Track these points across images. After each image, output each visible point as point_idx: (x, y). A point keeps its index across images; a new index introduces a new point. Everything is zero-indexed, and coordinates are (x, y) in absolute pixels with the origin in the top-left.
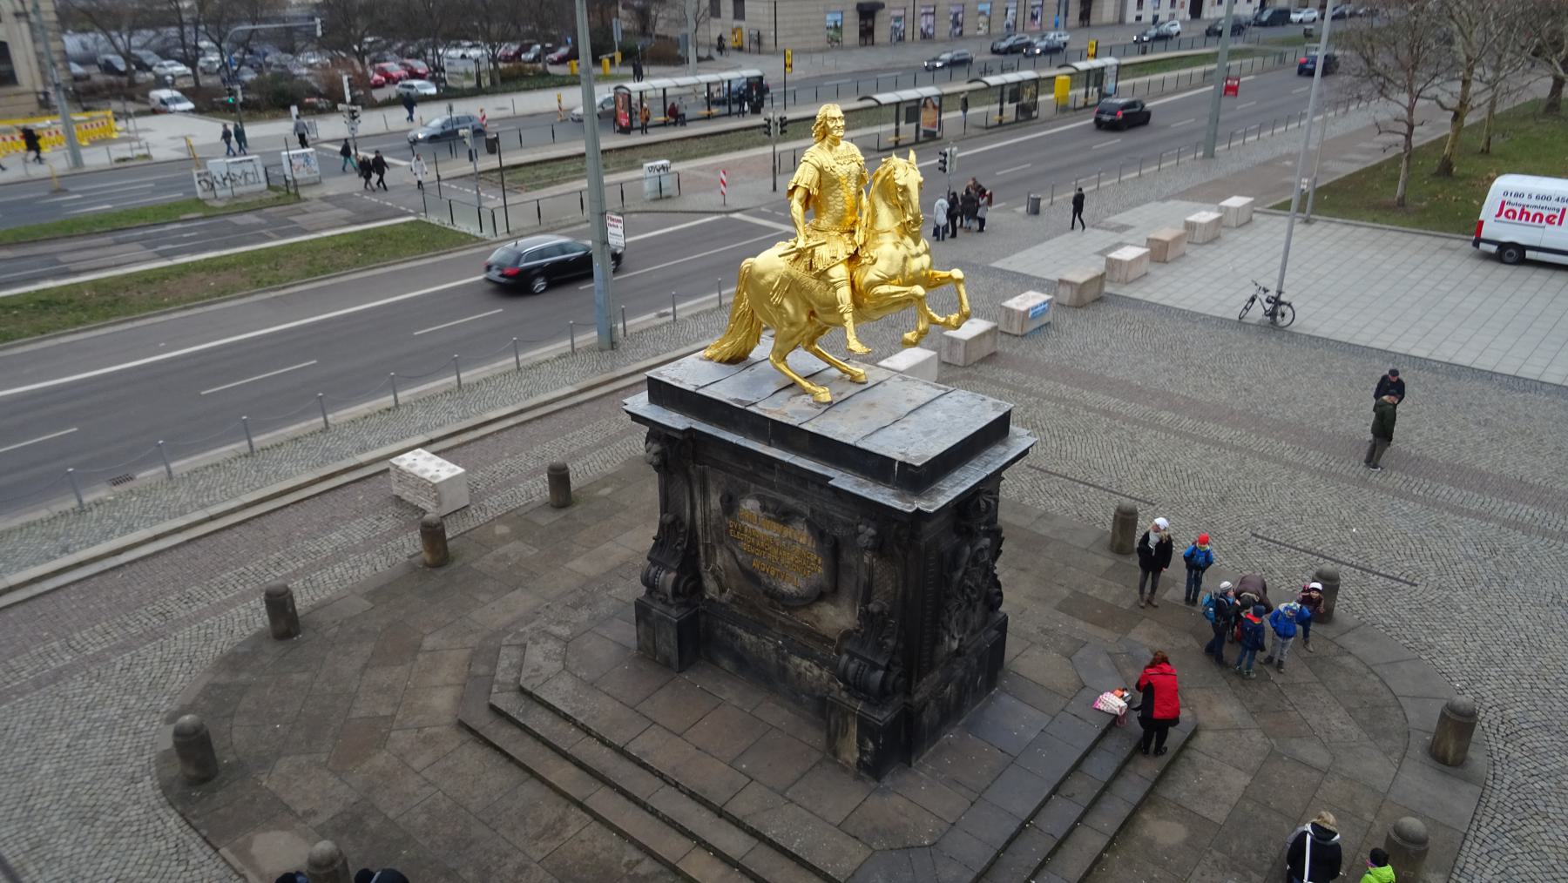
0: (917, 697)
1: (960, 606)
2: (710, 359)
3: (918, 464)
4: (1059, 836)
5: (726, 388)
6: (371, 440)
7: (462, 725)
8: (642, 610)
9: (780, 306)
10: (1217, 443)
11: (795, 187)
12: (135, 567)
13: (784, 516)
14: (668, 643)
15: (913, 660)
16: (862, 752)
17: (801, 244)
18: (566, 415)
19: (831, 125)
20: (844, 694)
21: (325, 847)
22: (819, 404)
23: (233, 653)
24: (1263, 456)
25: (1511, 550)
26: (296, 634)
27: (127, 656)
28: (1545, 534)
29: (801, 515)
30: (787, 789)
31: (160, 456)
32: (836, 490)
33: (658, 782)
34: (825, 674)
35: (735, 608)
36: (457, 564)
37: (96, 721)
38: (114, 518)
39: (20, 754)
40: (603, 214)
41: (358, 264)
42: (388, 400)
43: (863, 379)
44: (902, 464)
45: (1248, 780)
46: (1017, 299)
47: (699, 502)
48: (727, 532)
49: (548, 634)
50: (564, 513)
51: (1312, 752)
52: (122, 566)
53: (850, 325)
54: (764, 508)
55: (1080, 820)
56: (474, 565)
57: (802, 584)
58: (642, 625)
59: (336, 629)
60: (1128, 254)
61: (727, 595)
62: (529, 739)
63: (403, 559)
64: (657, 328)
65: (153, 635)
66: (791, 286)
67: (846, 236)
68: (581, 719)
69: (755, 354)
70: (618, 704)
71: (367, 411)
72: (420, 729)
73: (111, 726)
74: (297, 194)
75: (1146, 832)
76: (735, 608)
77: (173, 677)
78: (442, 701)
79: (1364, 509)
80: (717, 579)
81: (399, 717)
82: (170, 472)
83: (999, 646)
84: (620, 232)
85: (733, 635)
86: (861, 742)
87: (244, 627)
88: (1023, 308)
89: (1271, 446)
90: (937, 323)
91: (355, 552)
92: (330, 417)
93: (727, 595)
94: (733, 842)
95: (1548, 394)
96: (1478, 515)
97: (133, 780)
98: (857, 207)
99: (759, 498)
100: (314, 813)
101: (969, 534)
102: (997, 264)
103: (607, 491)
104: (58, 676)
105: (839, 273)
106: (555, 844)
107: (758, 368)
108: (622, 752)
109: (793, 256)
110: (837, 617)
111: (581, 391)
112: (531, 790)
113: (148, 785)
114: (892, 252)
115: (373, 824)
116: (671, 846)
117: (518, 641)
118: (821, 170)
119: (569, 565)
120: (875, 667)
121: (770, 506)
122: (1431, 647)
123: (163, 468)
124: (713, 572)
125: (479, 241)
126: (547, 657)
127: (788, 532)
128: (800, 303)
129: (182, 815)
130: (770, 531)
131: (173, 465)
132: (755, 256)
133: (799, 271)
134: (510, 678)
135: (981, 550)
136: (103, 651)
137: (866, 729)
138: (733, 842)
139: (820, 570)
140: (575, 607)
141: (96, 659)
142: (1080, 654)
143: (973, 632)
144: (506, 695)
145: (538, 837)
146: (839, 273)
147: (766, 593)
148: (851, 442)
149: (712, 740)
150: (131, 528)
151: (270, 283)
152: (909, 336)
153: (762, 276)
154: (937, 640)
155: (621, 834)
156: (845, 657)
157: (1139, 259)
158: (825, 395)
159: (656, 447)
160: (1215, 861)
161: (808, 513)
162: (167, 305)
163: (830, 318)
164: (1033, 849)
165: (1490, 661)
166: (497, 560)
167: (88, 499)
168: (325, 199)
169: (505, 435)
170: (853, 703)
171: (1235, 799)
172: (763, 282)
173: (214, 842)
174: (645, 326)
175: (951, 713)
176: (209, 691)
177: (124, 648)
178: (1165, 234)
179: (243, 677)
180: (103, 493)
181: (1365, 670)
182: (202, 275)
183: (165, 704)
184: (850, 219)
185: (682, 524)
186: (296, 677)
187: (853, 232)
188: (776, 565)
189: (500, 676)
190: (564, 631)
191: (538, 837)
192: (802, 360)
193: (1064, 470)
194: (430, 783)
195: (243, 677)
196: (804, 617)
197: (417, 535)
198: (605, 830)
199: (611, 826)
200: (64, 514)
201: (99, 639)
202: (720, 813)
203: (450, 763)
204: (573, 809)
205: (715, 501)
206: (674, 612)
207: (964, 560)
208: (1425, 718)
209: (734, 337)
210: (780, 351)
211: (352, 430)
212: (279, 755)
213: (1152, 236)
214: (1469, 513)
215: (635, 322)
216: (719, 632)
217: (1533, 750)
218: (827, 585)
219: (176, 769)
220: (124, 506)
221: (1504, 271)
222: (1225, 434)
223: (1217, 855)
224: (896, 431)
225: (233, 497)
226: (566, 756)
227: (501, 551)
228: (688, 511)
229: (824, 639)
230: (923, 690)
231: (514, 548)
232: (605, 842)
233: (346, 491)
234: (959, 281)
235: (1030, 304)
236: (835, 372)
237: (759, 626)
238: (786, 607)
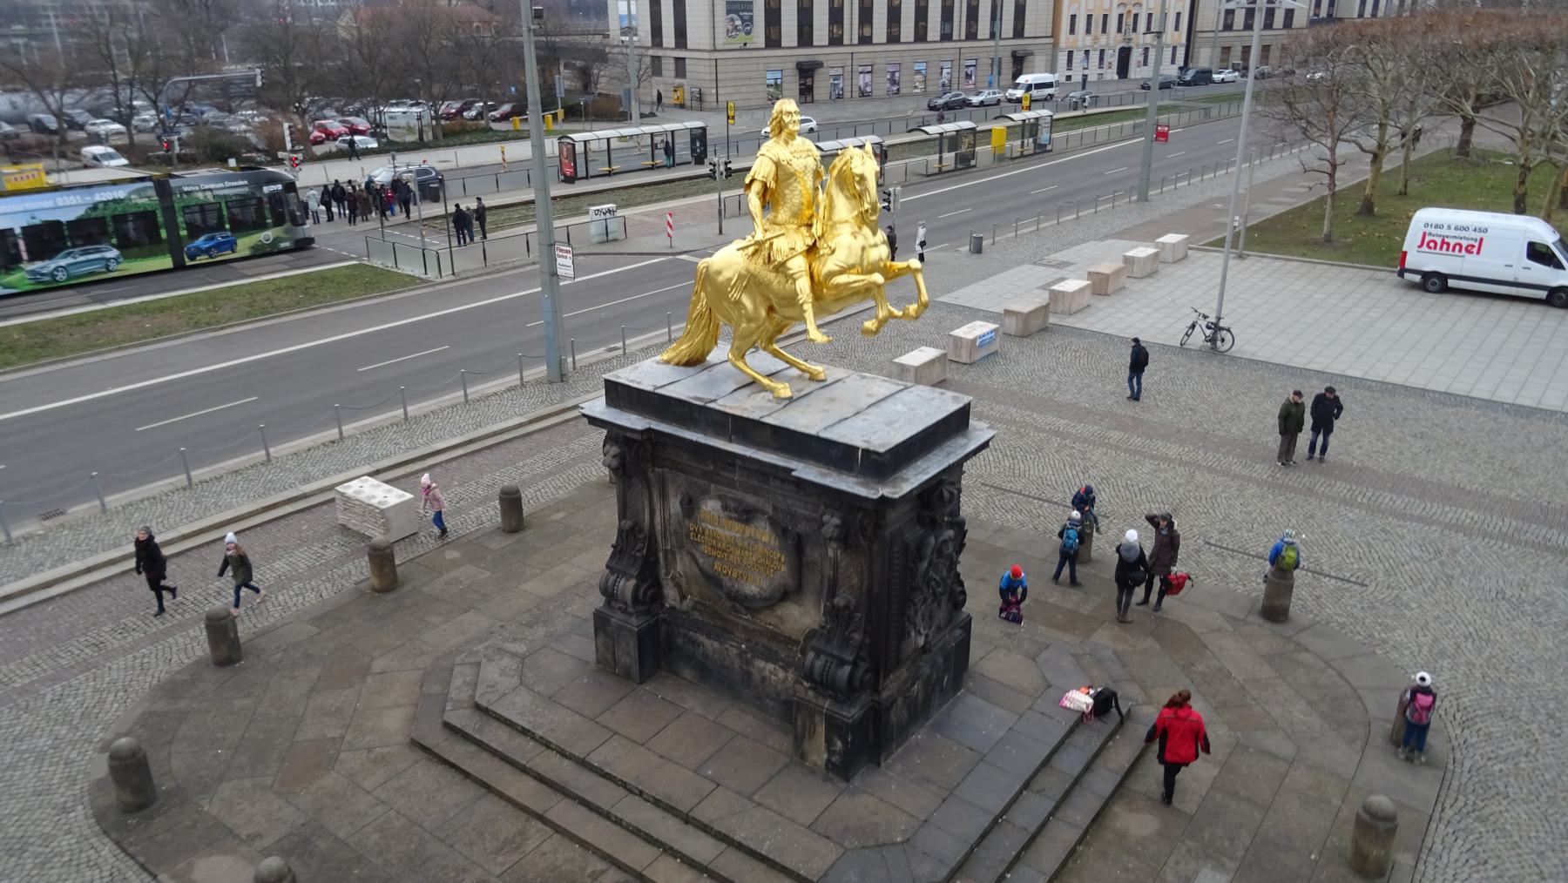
0: (885, 695)
1: (925, 600)
2: (667, 362)
3: (882, 450)
4: (1033, 829)
5: (685, 388)
6: (314, 471)
7: (416, 745)
8: (600, 620)
9: (738, 303)
10: (1166, 459)
11: (752, 181)
12: (66, 600)
13: (746, 515)
14: (628, 655)
15: (880, 655)
16: (831, 752)
17: (759, 236)
18: (516, 445)
19: (787, 119)
20: (811, 693)
21: (273, 863)
22: (779, 399)
24: (1210, 470)
25: (1453, 551)
26: (239, 660)
27: (58, 688)
29: (763, 512)
30: (754, 793)
31: (95, 490)
32: (801, 483)
33: (622, 791)
34: (791, 676)
35: (696, 615)
36: (407, 588)
37: (24, 752)
38: (44, 551)
40: (552, 245)
42: (333, 433)
43: (822, 376)
44: (866, 452)
45: (1216, 772)
47: (658, 507)
48: (688, 535)
49: (502, 651)
50: (516, 537)
51: (1276, 743)
52: (52, 598)
53: (809, 315)
54: (725, 508)
55: (1052, 814)
56: (425, 589)
57: (765, 584)
58: (601, 638)
59: (279, 655)
60: (1071, 285)
61: (688, 603)
62: (485, 755)
63: (349, 585)
65: (87, 666)
66: (750, 282)
67: (803, 229)
68: (539, 733)
69: (712, 357)
70: (577, 717)
71: (310, 444)
72: (370, 750)
73: (41, 757)
75: (1118, 825)
76: (696, 615)
77: (107, 706)
78: (394, 722)
79: (1312, 517)
80: (678, 586)
81: (348, 738)
82: (103, 505)
83: (964, 646)
84: (569, 262)
85: (695, 643)
86: (829, 742)
87: (183, 656)
88: (971, 337)
90: (895, 317)
91: (300, 580)
92: (271, 450)
93: (688, 603)
94: (701, 847)
95: (1478, 408)
96: (1420, 519)
97: (64, 810)
98: (814, 202)
99: (720, 498)
100: (259, 836)
101: (933, 525)
102: (944, 299)
103: (561, 515)
105: (798, 264)
106: (515, 858)
107: (715, 370)
108: (583, 763)
109: (751, 250)
110: (802, 617)
111: (531, 422)
112: (488, 805)
113: (80, 816)
114: (852, 244)
116: (637, 855)
117: (472, 660)
118: (777, 164)
119: (524, 587)
120: (842, 663)
121: (732, 505)
122: (1384, 642)
123: (97, 502)
124: (673, 579)
126: (503, 673)
128: (759, 299)
129: (117, 843)
130: (731, 531)
131: (107, 499)
132: (710, 255)
133: (757, 266)
134: (465, 695)
135: (945, 542)
136: (33, 682)
138: (701, 847)
139: (784, 568)
140: (530, 625)
141: (23, 691)
142: (1045, 655)
143: (939, 629)
144: (460, 712)
145: (497, 852)
146: (798, 264)
147: (728, 596)
148: (813, 432)
149: (675, 746)
150: (62, 561)
151: (208, 324)
152: (870, 324)
153: (719, 273)
154: (903, 635)
155: (585, 845)
156: (811, 655)
157: (1081, 290)
158: (785, 391)
159: (614, 450)
160: (1189, 850)
161: (770, 510)
162: (101, 346)
163: (789, 312)
164: (1007, 843)
165: (1442, 653)
166: (448, 583)
167: (16, 533)
169: (454, 464)
170: (820, 701)
171: (1204, 792)
172: (721, 278)
173: (152, 869)
175: (919, 712)
176: (146, 720)
177: (54, 680)
178: (1106, 268)
179: (182, 704)
180: (33, 527)
181: (1322, 665)
182: (136, 318)
183: (98, 734)
184: (807, 213)
185: (641, 530)
186: (238, 703)
187: (810, 226)
188: (738, 566)
189: (453, 694)
190: (521, 648)
192: (760, 362)
193: (1019, 487)
194: (383, 803)
195: (182, 704)
196: (767, 619)
197: (364, 562)
198: (567, 842)
199: (573, 838)
201: (28, 671)
202: (687, 819)
203: (402, 782)
204: (534, 822)
205: (675, 505)
206: (634, 621)
207: (929, 551)
208: (1385, 711)
209: (692, 338)
210: (738, 348)
211: (295, 463)
212: (221, 779)
213: (1093, 270)
214: (1412, 518)
215: (584, 357)
216: (680, 641)
217: (1489, 736)
218: (791, 583)
219: (111, 796)
220: (55, 539)
221: (1429, 299)
222: (1174, 451)
223: (1190, 843)
224: (858, 422)
225: (170, 528)
226: (525, 770)
227: (452, 575)
228: (647, 516)
229: (788, 641)
230: (892, 685)
233: (290, 521)
234: (917, 270)
235: (978, 332)
236: (794, 372)
237: (722, 632)
238: (749, 610)
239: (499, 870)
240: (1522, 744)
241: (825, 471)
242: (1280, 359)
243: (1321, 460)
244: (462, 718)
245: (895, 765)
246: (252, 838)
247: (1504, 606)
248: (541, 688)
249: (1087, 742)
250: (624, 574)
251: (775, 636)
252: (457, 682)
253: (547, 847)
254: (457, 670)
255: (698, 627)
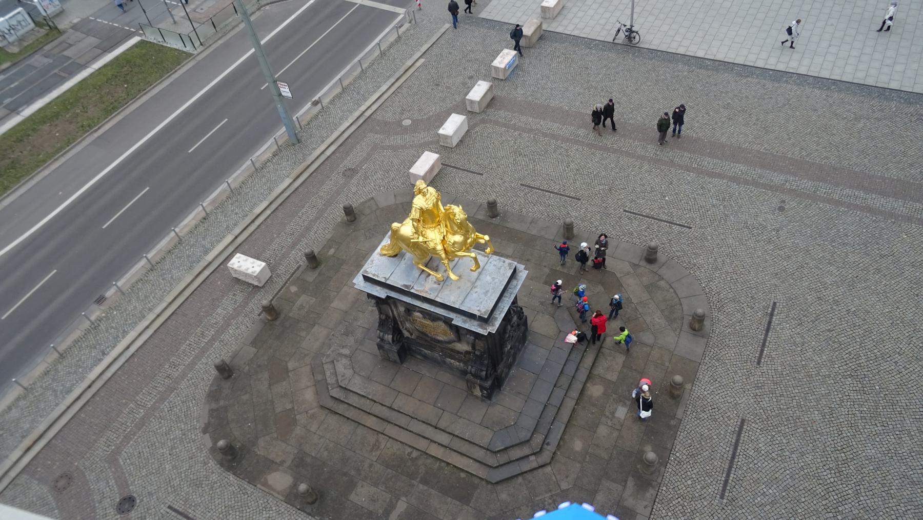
0: (499, 371)
2: (385, 255)
6: (207, 243)
14: (394, 356)
23: (211, 391)
24: (628, 154)
28: (746, 182)
36: (282, 316)
37: (173, 439)
38: (112, 327)
39: (153, 463)
41: (131, 96)
46: (498, 59)
50: (317, 271)
56: (291, 315)
59: (247, 368)
64: (316, 117)
72: (307, 412)
74: (56, 28)
75: (589, 393)
78: (309, 395)
80: (408, 331)
86: (481, 391)
88: (503, 66)
89: (631, 146)
92: (177, 230)
97: (205, 464)
103: (332, 251)
104: (143, 422)
106: (379, 452)
112: (360, 431)
113: (212, 463)
115: (308, 460)
117: (328, 360)
119: (332, 305)
125: (189, 55)
127: (436, 324)
137: (482, 388)
140: (347, 334)
141: (154, 408)
145: (371, 451)
146: (439, 247)
150: (125, 333)
151: (90, 126)
162: (44, 161)
165: (716, 269)
166: (299, 309)
167: (93, 318)
168: (75, 27)
174: (308, 118)
177: (162, 399)
179: (222, 403)
181: (668, 287)
182: (46, 127)
189: (329, 381)
191: (371, 451)
193: (537, 184)
194: (322, 437)
195: (222, 403)
200: (88, 331)
212: (257, 438)
227: (298, 303)
229: (458, 352)
230: (501, 368)
231: (304, 299)
232: (397, 446)
237: (431, 348)
239: (375, 459)
240: (739, 316)
241: (465, 318)
242: (663, 48)
243: (679, 137)
244: (336, 393)
245: (506, 388)
246: (283, 462)
247: (746, 231)
248: (363, 374)
249: (576, 357)
250: (385, 333)
251: (452, 350)
252: (328, 374)
253: (389, 445)
254: (325, 366)
255: (421, 345)
